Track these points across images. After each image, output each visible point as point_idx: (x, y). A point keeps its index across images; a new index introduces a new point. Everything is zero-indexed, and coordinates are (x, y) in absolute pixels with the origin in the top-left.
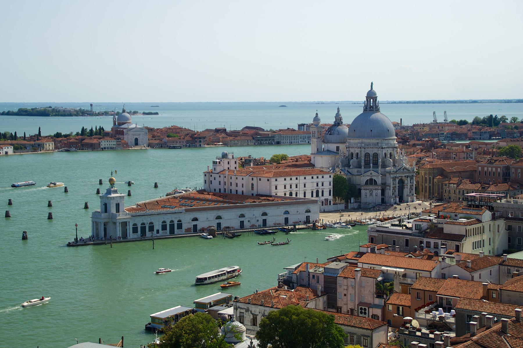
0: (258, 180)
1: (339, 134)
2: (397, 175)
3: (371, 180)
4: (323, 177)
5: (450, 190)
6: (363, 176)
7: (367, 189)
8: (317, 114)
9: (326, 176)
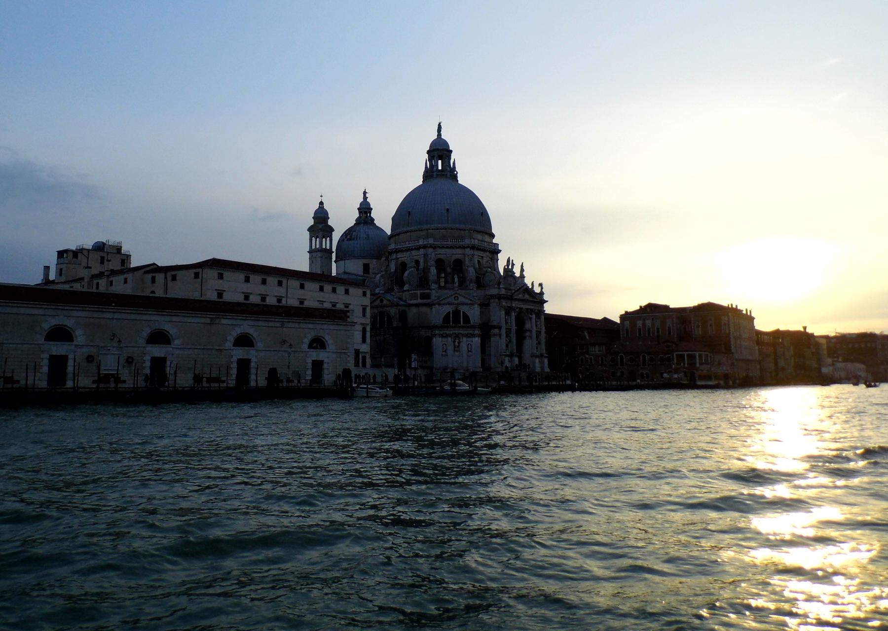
0: (169, 278)
1: (368, 238)
2: (514, 305)
3: (456, 312)
4: (347, 292)
5: (591, 359)
6: (439, 304)
7: (447, 336)
8: (321, 203)
9: (355, 291)
